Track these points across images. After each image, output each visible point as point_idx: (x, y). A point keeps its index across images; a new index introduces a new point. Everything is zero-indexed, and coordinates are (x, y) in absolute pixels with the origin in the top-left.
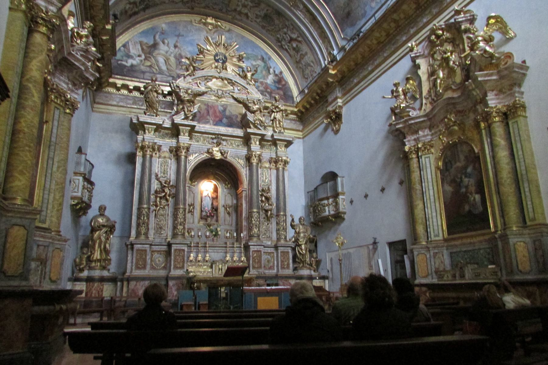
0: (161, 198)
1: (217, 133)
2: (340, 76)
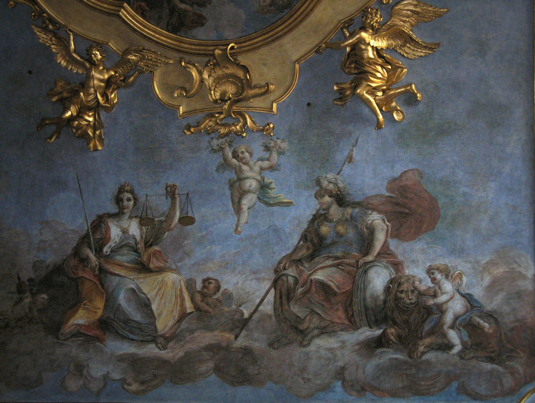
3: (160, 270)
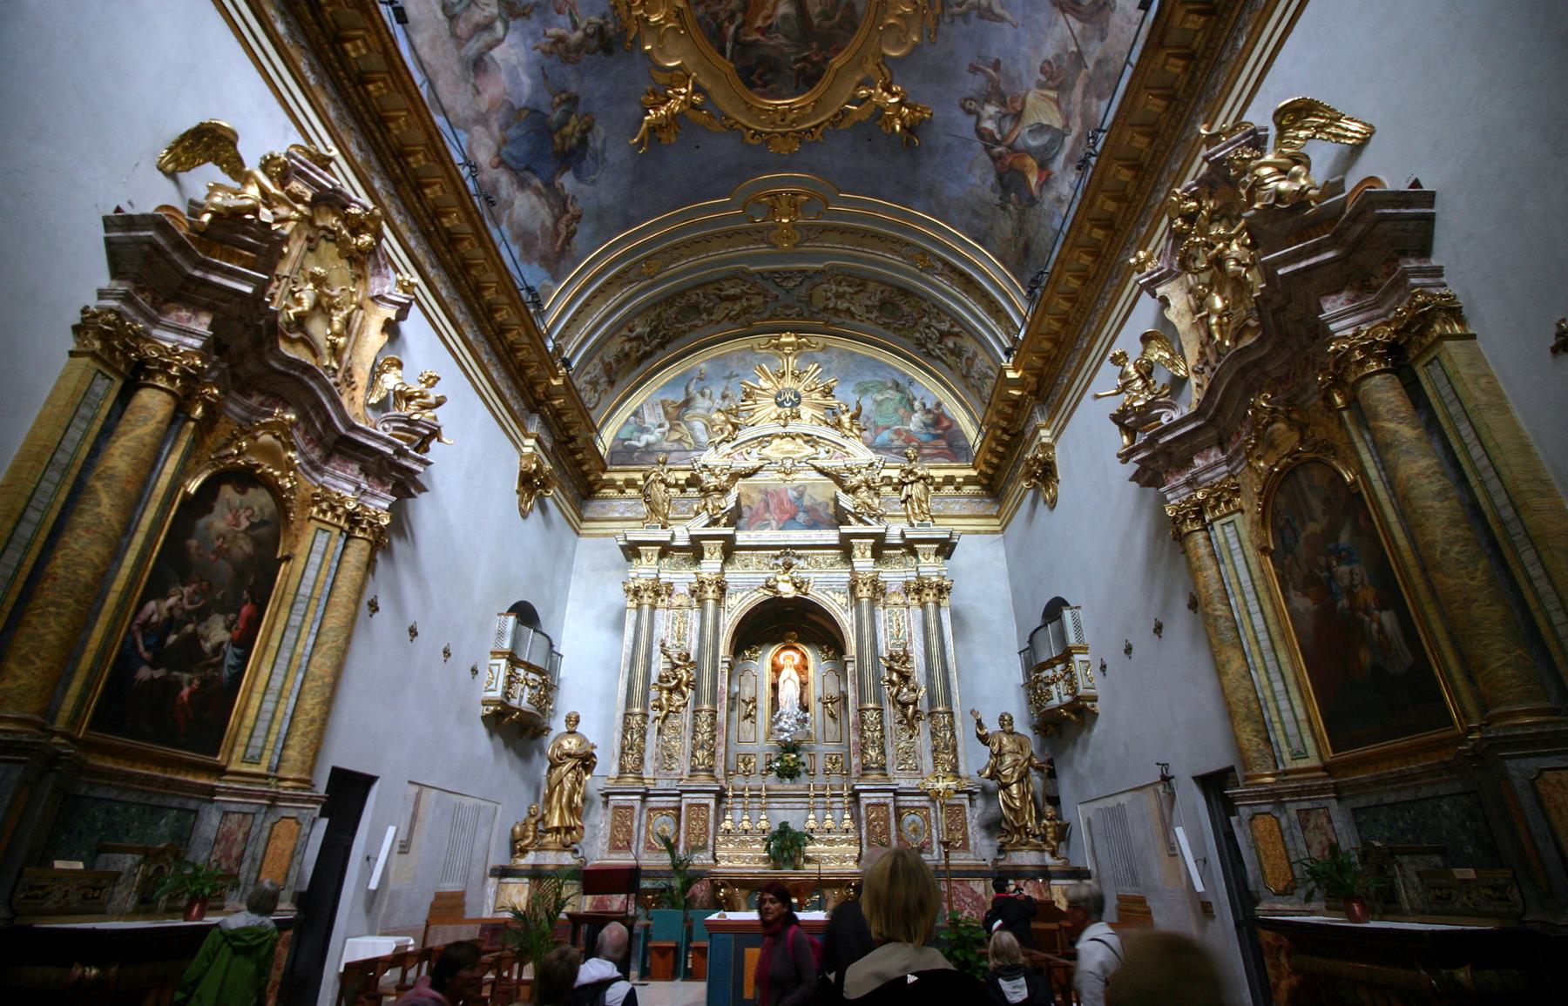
0: (670, 691)
2: (1032, 380)
3: (1024, 103)
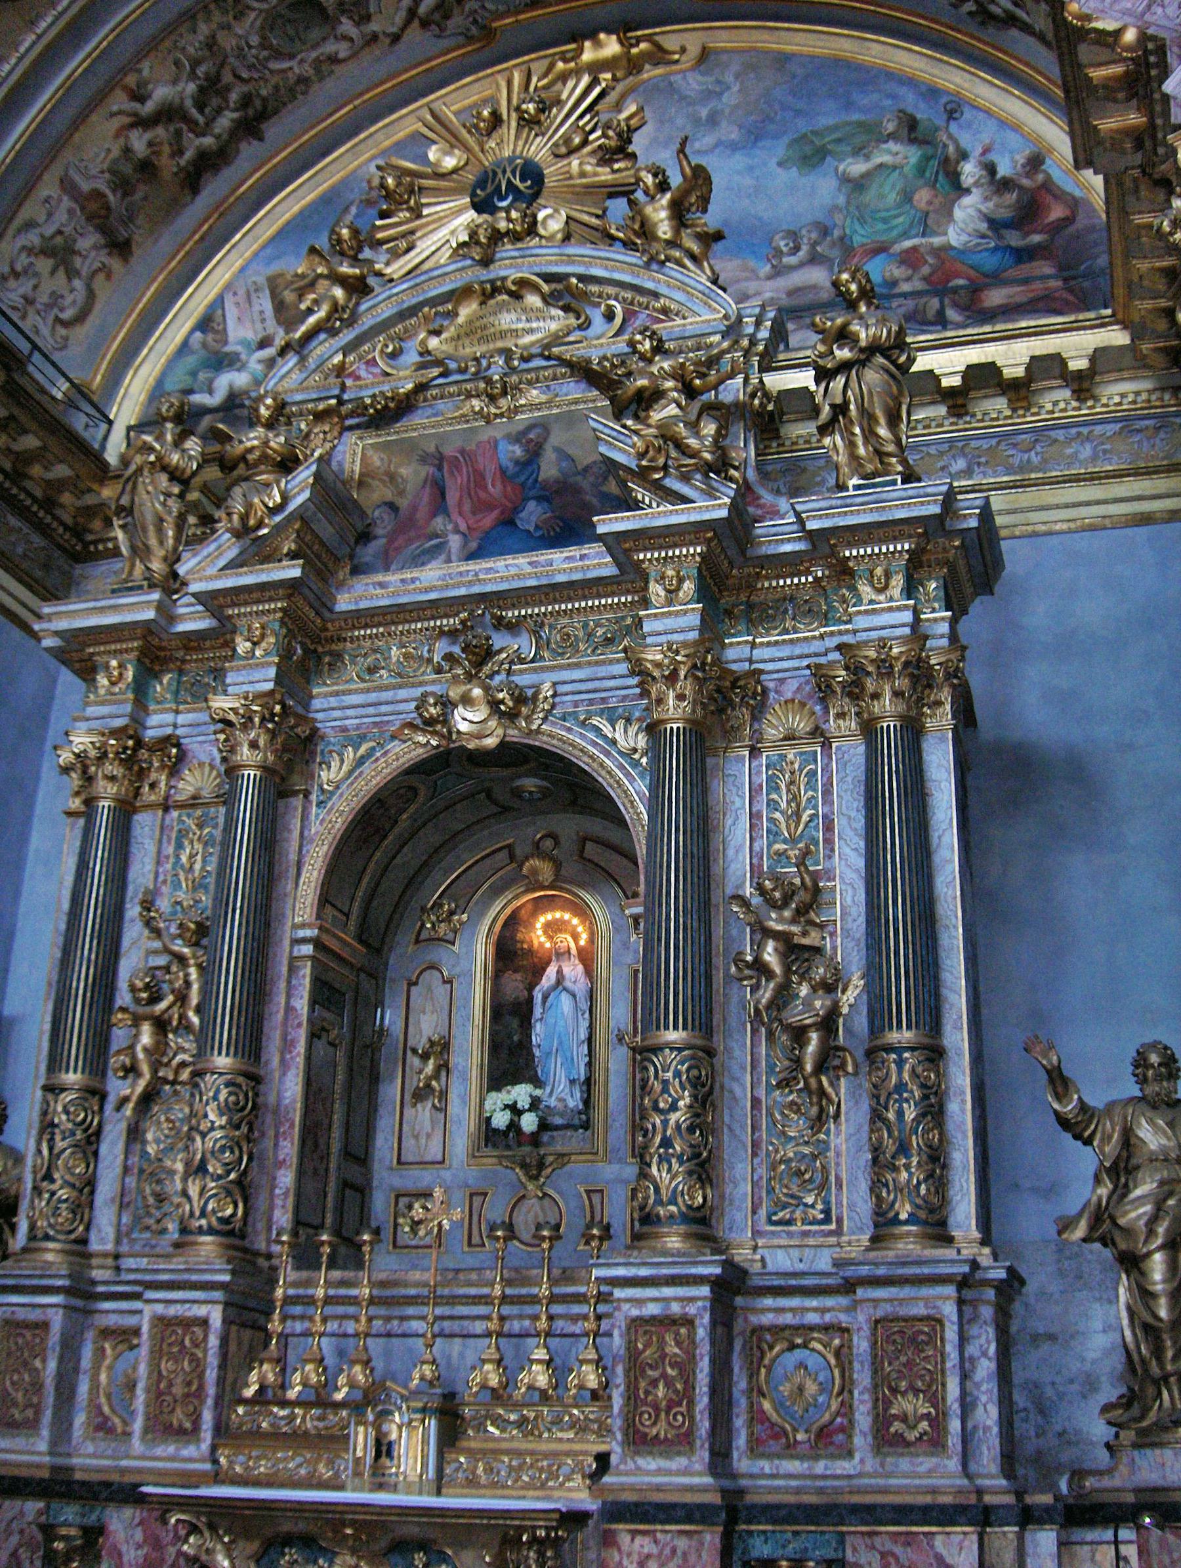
1: (463, 591)
